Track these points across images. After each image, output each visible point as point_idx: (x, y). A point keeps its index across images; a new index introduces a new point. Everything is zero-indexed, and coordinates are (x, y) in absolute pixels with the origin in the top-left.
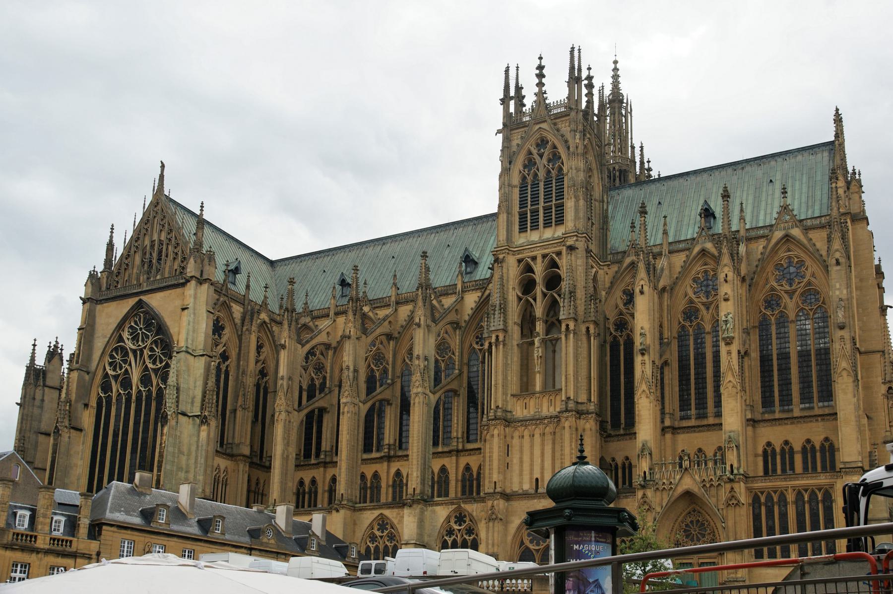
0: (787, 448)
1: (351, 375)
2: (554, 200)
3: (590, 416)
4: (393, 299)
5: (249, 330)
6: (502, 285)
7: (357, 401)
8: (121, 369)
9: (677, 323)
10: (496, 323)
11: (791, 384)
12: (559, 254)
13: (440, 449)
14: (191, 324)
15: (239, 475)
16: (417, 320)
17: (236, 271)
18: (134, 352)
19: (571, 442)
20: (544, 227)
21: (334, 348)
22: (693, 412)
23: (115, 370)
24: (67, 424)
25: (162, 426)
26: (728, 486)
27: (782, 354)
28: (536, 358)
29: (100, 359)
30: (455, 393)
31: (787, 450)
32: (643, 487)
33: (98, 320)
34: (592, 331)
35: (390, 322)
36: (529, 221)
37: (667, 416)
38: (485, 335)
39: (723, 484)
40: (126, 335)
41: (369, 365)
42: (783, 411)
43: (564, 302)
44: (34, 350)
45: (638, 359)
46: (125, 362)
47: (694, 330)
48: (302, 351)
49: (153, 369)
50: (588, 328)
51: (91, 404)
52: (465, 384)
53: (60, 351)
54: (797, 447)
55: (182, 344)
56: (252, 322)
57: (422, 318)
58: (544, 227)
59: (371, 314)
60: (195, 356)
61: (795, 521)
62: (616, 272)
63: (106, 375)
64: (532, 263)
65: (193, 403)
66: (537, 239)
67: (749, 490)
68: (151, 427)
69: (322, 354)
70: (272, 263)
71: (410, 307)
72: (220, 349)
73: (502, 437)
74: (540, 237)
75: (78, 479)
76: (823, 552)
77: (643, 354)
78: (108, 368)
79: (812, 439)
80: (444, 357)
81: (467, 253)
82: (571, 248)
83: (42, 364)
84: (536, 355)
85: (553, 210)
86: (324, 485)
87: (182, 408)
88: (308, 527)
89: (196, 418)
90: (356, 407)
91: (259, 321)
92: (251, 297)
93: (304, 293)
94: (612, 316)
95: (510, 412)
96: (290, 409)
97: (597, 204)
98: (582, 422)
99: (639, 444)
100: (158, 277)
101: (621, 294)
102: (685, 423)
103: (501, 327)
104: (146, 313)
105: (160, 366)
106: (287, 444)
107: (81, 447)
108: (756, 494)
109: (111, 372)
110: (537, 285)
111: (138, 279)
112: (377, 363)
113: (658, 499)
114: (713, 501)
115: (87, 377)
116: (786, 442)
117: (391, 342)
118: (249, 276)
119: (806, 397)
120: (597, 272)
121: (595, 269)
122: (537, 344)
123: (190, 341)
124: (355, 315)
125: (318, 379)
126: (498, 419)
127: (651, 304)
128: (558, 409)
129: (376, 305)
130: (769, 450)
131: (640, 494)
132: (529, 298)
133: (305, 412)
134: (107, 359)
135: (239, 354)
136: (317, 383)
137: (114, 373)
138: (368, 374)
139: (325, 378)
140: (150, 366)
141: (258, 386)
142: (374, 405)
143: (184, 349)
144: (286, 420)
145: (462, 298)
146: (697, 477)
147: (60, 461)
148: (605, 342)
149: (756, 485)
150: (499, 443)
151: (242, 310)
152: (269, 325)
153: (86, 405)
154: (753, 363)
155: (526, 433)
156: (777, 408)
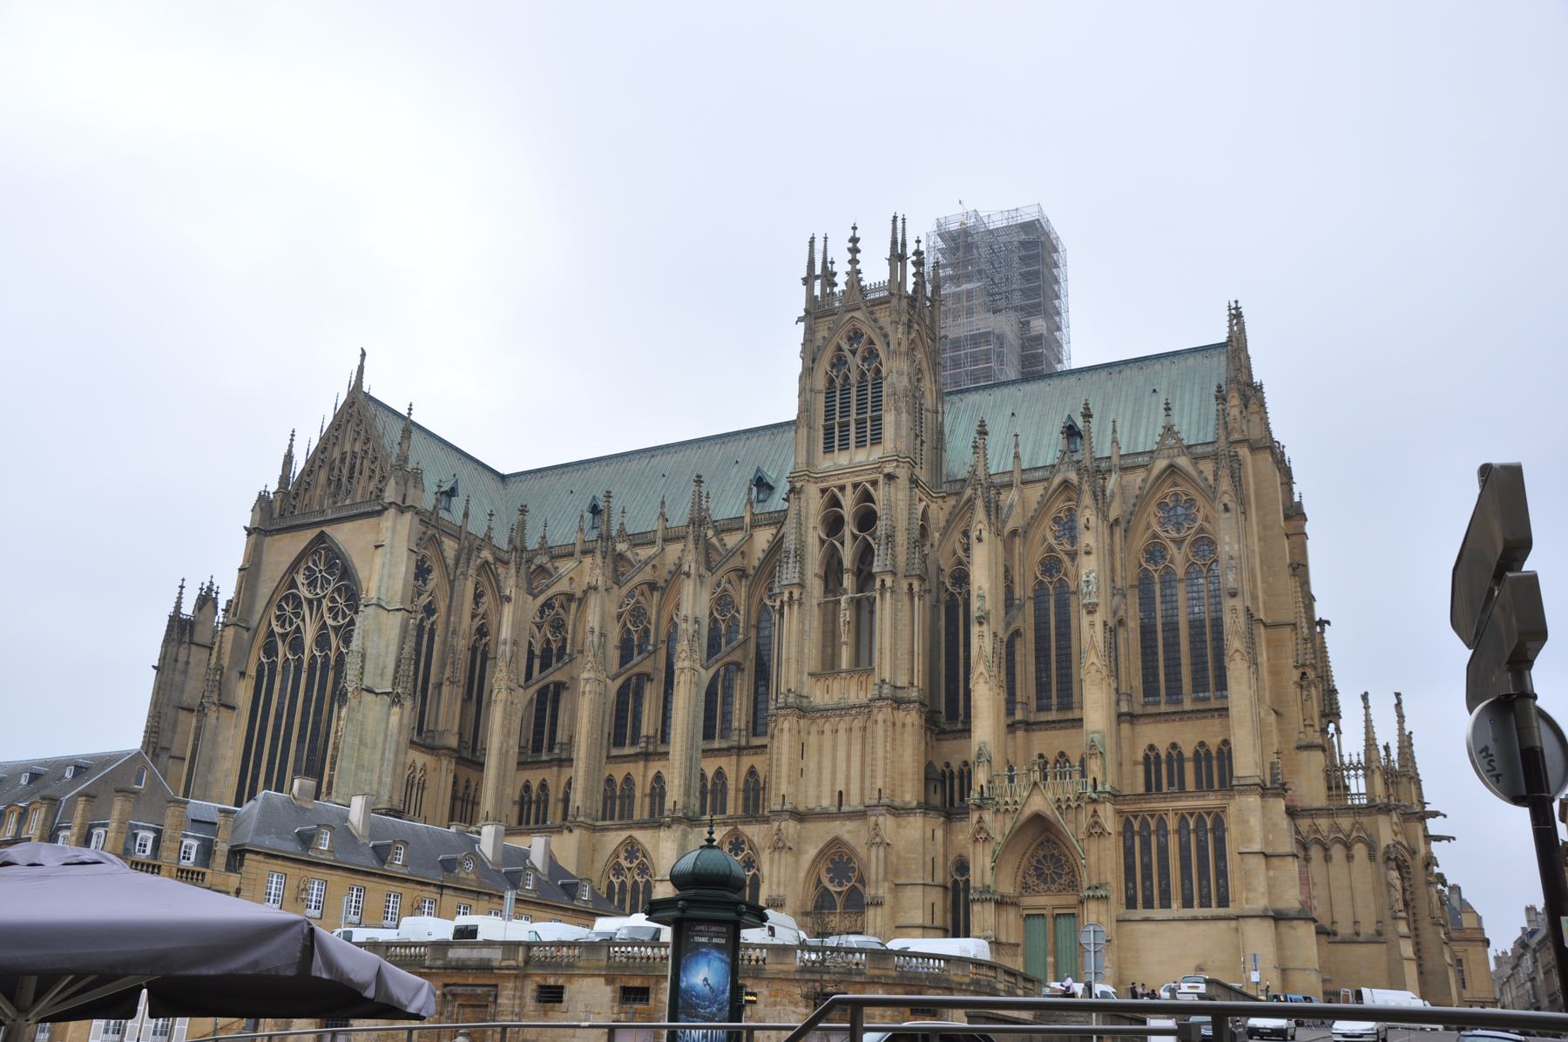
0: (1174, 753)
1: (596, 640)
2: (869, 409)
4: (659, 534)
5: (464, 574)
6: (799, 524)
7: (603, 677)
8: (291, 625)
9: (1033, 578)
10: (789, 574)
11: (1180, 665)
12: (874, 483)
13: (716, 744)
14: (386, 566)
15: (441, 777)
16: (686, 568)
17: (451, 493)
18: (310, 602)
19: (885, 742)
20: (857, 447)
21: (579, 599)
22: (1054, 700)
23: (283, 626)
24: (215, 699)
25: (340, 707)
26: (1090, 808)
28: (842, 623)
29: (265, 610)
30: (739, 667)
31: (1175, 757)
32: (980, 807)
33: (265, 556)
34: (916, 588)
35: (654, 566)
36: (837, 438)
37: (1019, 706)
38: (777, 590)
39: (1083, 805)
40: (300, 579)
41: (625, 624)
42: (1168, 702)
43: (879, 550)
44: (181, 593)
45: (975, 630)
46: (297, 615)
47: (1055, 588)
48: (534, 605)
49: (334, 628)
50: (911, 585)
51: (248, 672)
52: (752, 654)
53: (214, 595)
54: (1188, 753)
55: (373, 594)
56: (469, 563)
57: (693, 565)
58: (857, 447)
59: (629, 554)
60: (389, 611)
61: (1178, 857)
62: (954, 507)
63: (271, 633)
64: (839, 495)
65: (382, 675)
66: (846, 463)
67: (1119, 813)
68: (326, 707)
69: (562, 606)
70: (503, 478)
71: (680, 546)
72: (424, 599)
73: (795, 732)
74: (851, 460)
75: (226, 776)
76: (1213, 903)
77: (981, 624)
78: (274, 623)
80: (725, 615)
81: (759, 474)
82: (890, 477)
83: (190, 613)
84: (842, 620)
85: (869, 424)
86: (557, 792)
87: (368, 682)
88: (525, 855)
89: (385, 697)
90: (602, 685)
91: (479, 560)
92: (470, 528)
93: (542, 522)
94: (948, 565)
95: (807, 697)
96: (513, 685)
97: (929, 415)
99: (975, 749)
100: (348, 502)
102: (1044, 717)
103: (796, 581)
104: (328, 549)
105: (342, 622)
106: (507, 735)
107: (232, 732)
108: (1128, 819)
109: (278, 630)
110: (846, 524)
111: (321, 504)
112: (635, 622)
113: (998, 825)
114: (1068, 829)
115: (246, 635)
116: (1174, 746)
117: (655, 594)
118: (468, 501)
119: (1199, 685)
120: (927, 506)
121: (924, 503)
122: (843, 604)
123: (383, 590)
124: (604, 558)
125: (555, 641)
126: (790, 708)
127: (993, 555)
128: (869, 696)
129: (637, 542)
130: (1152, 755)
131: (975, 817)
132: (836, 542)
133: (537, 687)
134: (275, 611)
135: (450, 607)
136: (554, 646)
137: (281, 631)
138: (622, 636)
139: (565, 639)
140: (330, 622)
141: (474, 650)
142: (629, 679)
143: (374, 601)
144: (506, 700)
145: (751, 535)
147: (204, 750)
148: (938, 601)
149: (1126, 807)
150: (790, 741)
151: (456, 546)
152: (493, 567)
153: (243, 674)
154: (1131, 635)
155: (828, 727)
156: (1163, 697)
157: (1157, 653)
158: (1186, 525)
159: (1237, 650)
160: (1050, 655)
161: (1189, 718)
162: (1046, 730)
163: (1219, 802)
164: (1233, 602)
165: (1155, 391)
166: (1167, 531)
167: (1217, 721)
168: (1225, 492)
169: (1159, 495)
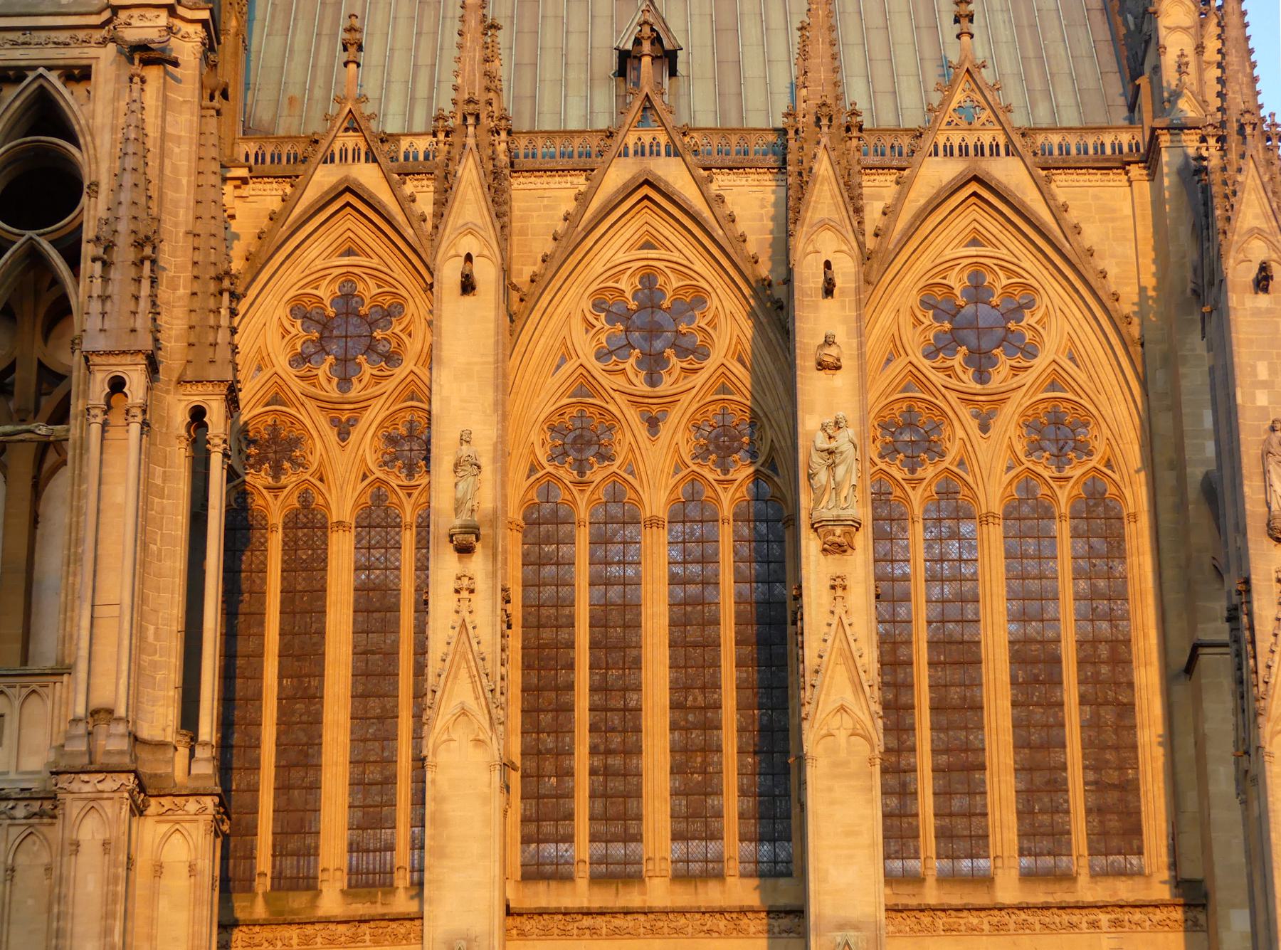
3: (192, 805)
9: (524, 468)
11: (982, 767)
22: (582, 848)
45: (446, 566)
50: (198, 414)
77: (464, 550)
98: (150, 831)
101: (283, 312)
161: (1024, 925)
162: (565, 934)
168: (1256, 232)
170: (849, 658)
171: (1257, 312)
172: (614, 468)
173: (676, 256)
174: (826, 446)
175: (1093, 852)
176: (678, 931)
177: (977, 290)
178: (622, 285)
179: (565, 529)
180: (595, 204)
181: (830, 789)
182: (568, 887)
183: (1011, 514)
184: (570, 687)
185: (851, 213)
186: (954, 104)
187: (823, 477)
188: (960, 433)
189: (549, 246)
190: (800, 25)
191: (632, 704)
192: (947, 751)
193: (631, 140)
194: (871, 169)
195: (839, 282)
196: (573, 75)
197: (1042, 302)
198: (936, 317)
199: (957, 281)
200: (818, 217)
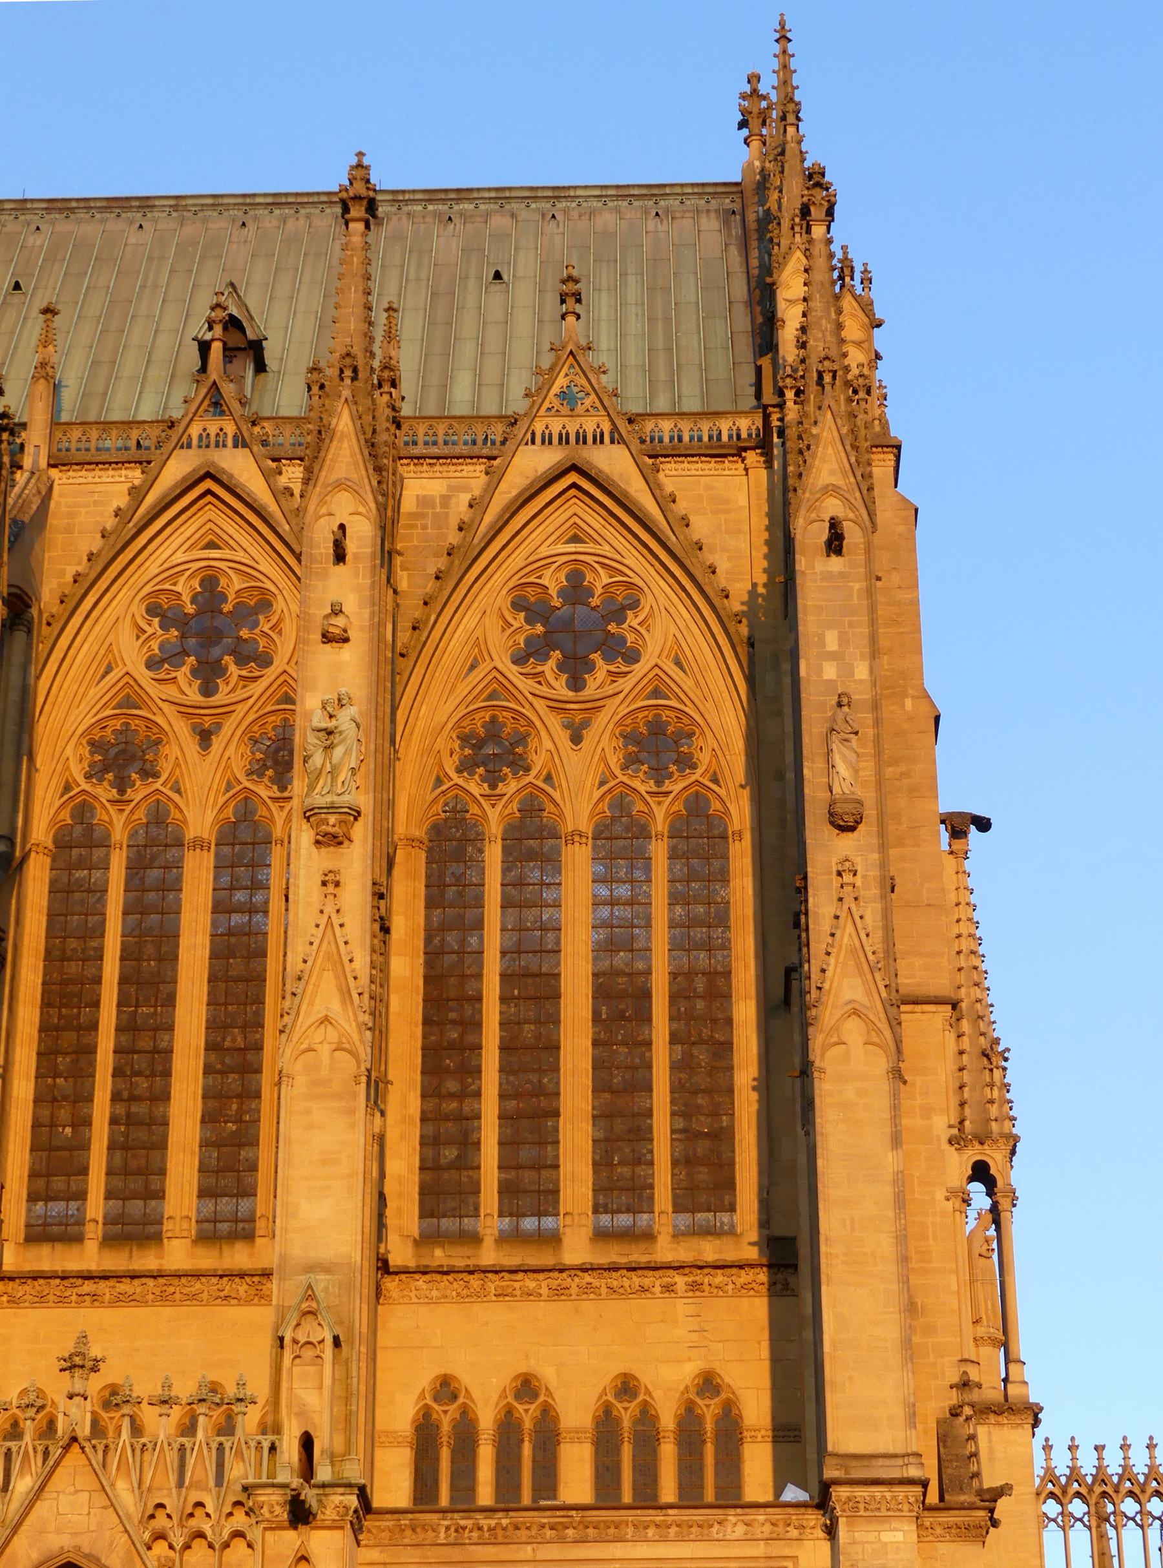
0: (527, 1414)
9: (56, 784)
11: (557, 1114)
22: (96, 1206)
27: (526, 974)
39: (255, 1534)
79: (646, 1376)
102: (47, 1258)
116: (527, 1387)
146: (124, 1492)
157: (477, 1071)
158: (602, 668)
159: (856, 1012)
160: (92, 1050)
161: (588, 1289)
162: (62, 1301)
163: (759, 1549)
164: (846, 844)
165: (498, 276)
166: (537, 676)
167: (682, 1307)
168: (830, 490)
169: (516, 560)
170: (339, 963)
171: (828, 576)
172: (158, 785)
173: (240, 556)
174: (323, 725)
175: (678, 1208)
176: (193, 1297)
177: (576, 589)
178: (178, 588)
179: (98, 853)
180: (150, 499)
181: (308, 1112)
182: (75, 1249)
183: (602, 833)
184: (94, 1026)
185: (371, 471)
186: (555, 389)
187: (318, 759)
188: (547, 744)
189: (96, 543)
190: (387, 306)
191: (163, 1045)
192: (516, 1096)
193: (195, 431)
194: (458, 458)
195: (351, 547)
196: (153, 373)
197: (647, 602)
198: (528, 621)
199: (553, 581)
200: (334, 477)
